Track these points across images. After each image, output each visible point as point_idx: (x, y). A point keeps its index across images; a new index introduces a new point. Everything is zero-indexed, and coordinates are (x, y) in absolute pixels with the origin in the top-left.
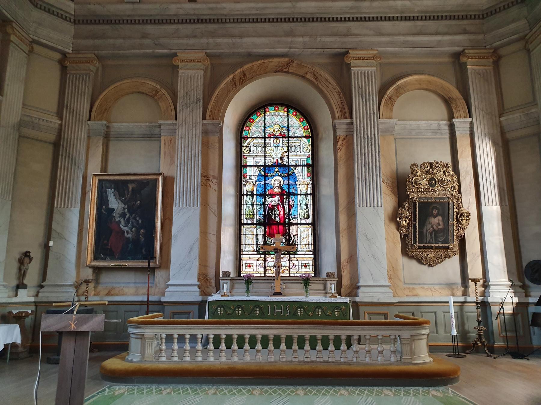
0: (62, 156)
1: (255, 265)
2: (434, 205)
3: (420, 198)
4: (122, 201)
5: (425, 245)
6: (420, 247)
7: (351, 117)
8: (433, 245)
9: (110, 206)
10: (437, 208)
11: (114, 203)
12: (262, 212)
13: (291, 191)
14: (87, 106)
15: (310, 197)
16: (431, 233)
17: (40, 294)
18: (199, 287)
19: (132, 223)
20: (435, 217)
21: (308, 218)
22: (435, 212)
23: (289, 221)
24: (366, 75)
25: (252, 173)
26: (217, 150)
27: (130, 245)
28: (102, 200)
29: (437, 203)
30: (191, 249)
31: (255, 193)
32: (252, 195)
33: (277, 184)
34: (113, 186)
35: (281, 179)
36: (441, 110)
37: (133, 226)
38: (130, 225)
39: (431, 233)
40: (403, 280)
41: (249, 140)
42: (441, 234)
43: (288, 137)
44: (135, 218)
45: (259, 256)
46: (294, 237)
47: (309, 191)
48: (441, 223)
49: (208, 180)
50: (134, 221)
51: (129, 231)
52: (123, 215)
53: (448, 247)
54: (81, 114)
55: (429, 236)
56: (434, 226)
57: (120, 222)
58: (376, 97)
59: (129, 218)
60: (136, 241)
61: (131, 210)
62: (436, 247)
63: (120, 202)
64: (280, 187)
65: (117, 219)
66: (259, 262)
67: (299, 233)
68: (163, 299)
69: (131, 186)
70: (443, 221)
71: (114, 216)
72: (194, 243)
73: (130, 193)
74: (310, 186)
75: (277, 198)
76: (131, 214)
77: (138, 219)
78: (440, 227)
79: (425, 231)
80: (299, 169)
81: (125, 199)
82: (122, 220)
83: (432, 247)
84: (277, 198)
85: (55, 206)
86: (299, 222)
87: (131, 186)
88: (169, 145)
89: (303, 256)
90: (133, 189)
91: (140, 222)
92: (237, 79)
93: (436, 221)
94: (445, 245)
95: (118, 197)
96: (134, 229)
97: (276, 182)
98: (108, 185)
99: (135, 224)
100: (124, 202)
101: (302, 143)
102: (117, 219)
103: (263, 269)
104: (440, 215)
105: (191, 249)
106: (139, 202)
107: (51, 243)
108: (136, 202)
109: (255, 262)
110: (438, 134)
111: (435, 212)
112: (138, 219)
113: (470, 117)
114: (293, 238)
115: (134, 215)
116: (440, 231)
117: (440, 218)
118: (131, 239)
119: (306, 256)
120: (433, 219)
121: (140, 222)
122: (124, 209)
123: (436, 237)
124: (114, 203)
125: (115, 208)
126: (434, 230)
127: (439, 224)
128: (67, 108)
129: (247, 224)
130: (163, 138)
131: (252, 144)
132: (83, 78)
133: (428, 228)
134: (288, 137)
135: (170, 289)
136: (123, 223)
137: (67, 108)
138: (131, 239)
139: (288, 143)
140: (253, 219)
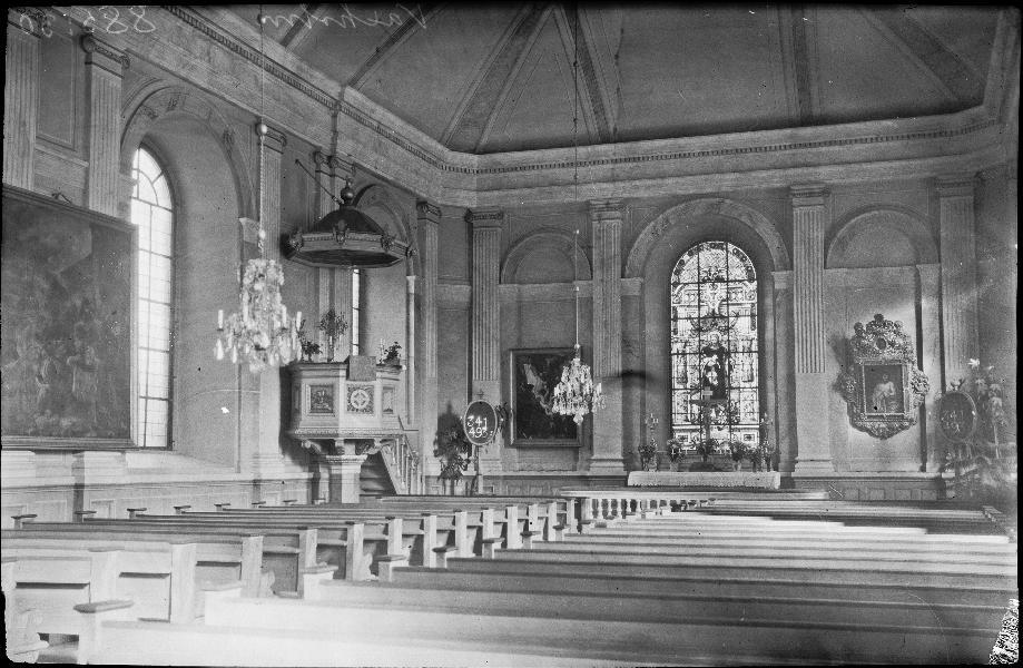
6: (869, 417)
7: (792, 269)
11: (532, 379)
12: (697, 374)
13: (732, 348)
14: (496, 267)
15: (755, 355)
20: (885, 383)
21: (752, 381)
23: (730, 384)
25: (684, 327)
27: (552, 424)
28: (520, 377)
31: (688, 350)
32: (684, 354)
33: (714, 340)
35: (716, 332)
43: (728, 281)
45: (692, 427)
47: (755, 348)
57: (539, 399)
58: (821, 246)
64: (718, 343)
74: (755, 342)
75: (715, 357)
80: (741, 320)
82: (542, 397)
84: (715, 357)
92: (659, 227)
97: (714, 338)
100: (543, 378)
116: (891, 398)
117: (891, 384)
124: (532, 379)
134: (728, 281)
136: (543, 400)
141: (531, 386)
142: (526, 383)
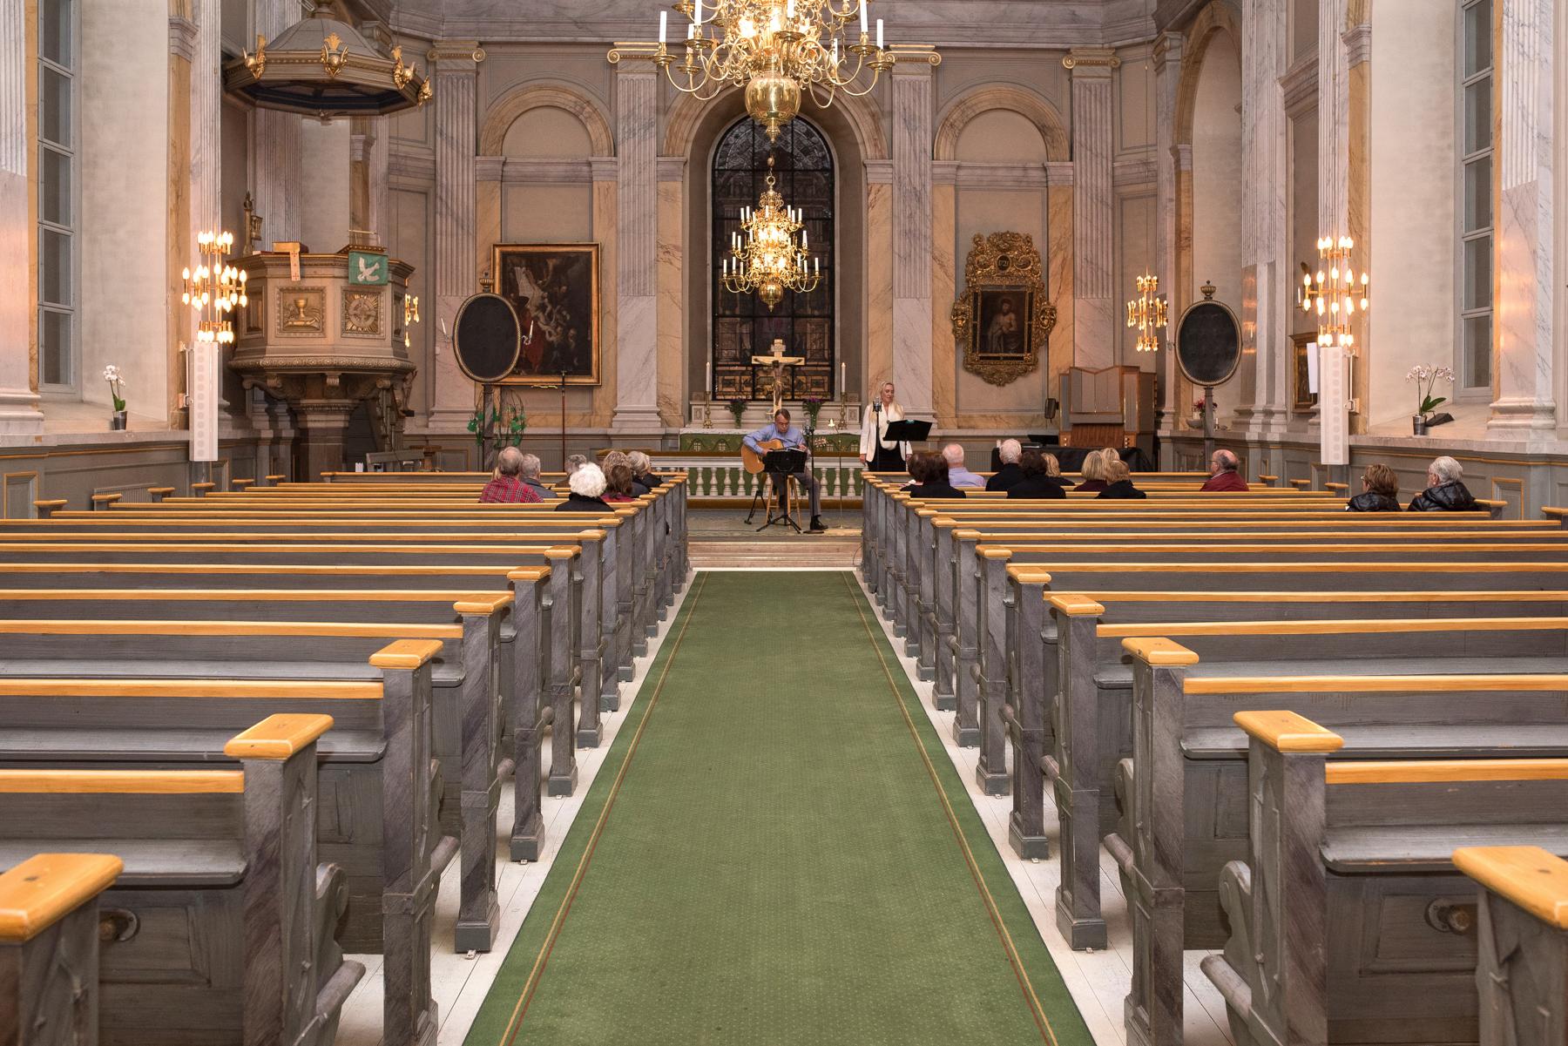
0: (441, 214)
1: (738, 381)
2: (1004, 297)
3: (982, 286)
4: (538, 285)
5: (991, 355)
6: (982, 358)
8: (1000, 354)
9: (521, 294)
10: (1008, 302)
16: (999, 338)
17: (431, 425)
18: (659, 414)
19: (556, 320)
20: (1005, 314)
22: (1006, 307)
24: (916, 88)
26: (680, 204)
27: (555, 353)
29: (1009, 293)
30: (647, 360)
34: (524, 262)
36: (1030, 145)
37: (558, 324)
38: (553, 324)
39: (999, 338)
40: (953, 404)
41: (728, 173)
42: (1013, 340)
44: (559, 312)
46: (800, 337)
48: (1014, 323)
49: (668, 252)
50: (558, 316)
51: (553, 332)
52: (542, 308)
53: (1022, 358)
54: (466, 146)
55: (995, 342)
56: (1004, 329)
57: (536, 319)
59: (551, 313)
60: (563, 346)
61: (553, 299)
62: (1006, 358)
63: (536, 288)
65: (533, 314)
66: (745, 378)
67: (809, 331)
68: (610, 431)
69: (551, 263)
70: (1016, 320)
71: (528, 310)
72: (651, 351)
73: (550, 273)
76: (554, 307)
77: (564, 313)
78: (1012, 329)
79: (990, 334)
81: (544, 283)
82: (541, 315)
83: (998, 358)
85: (438, 293)
86: (809, 312)
87: (551, 263)
88: (606, 196)
89: (815, 368)
90: (555, 268)
91: (568, 318)
93: (1006, 321)
94: (1018, 355)
95: (532, 280)
96: (559, 329)
98: (516, 260)
99: (561, 322)
101: (815, 181)
102: (533, 314)
103: (749, 389)
104: (1013, 312)
105: (647, 360)
106: (564, 288)
107: (438, 350)
108: (560, 288)
109: (738, 378)
110: (1024, 184)
111: (1006, 307)
112: (564, 313)
113: (1071, 160)
114: (798, 339)
115: (558, 307)
117: (1012, 316)
118: (556, 344)
119: (819, 369)
120: (1002, 317)
121: (568, 318)
122: (543, 298)
123: (1006, 344)
125: (530, 297)
126: (1003, 334)
127: (1011, 326)
128: (441, 134)
129: (724, 316)
130: (595, 185)
131: (732, 180)
132: (463, 83)
133: (995, 330)
135: (619, 417)
136: (542, 319)
137: (441, 134)
138: (556, 344)
139: (792, 180)
140: (733, 310)
141: (526, 300)
142: (517, 291)
